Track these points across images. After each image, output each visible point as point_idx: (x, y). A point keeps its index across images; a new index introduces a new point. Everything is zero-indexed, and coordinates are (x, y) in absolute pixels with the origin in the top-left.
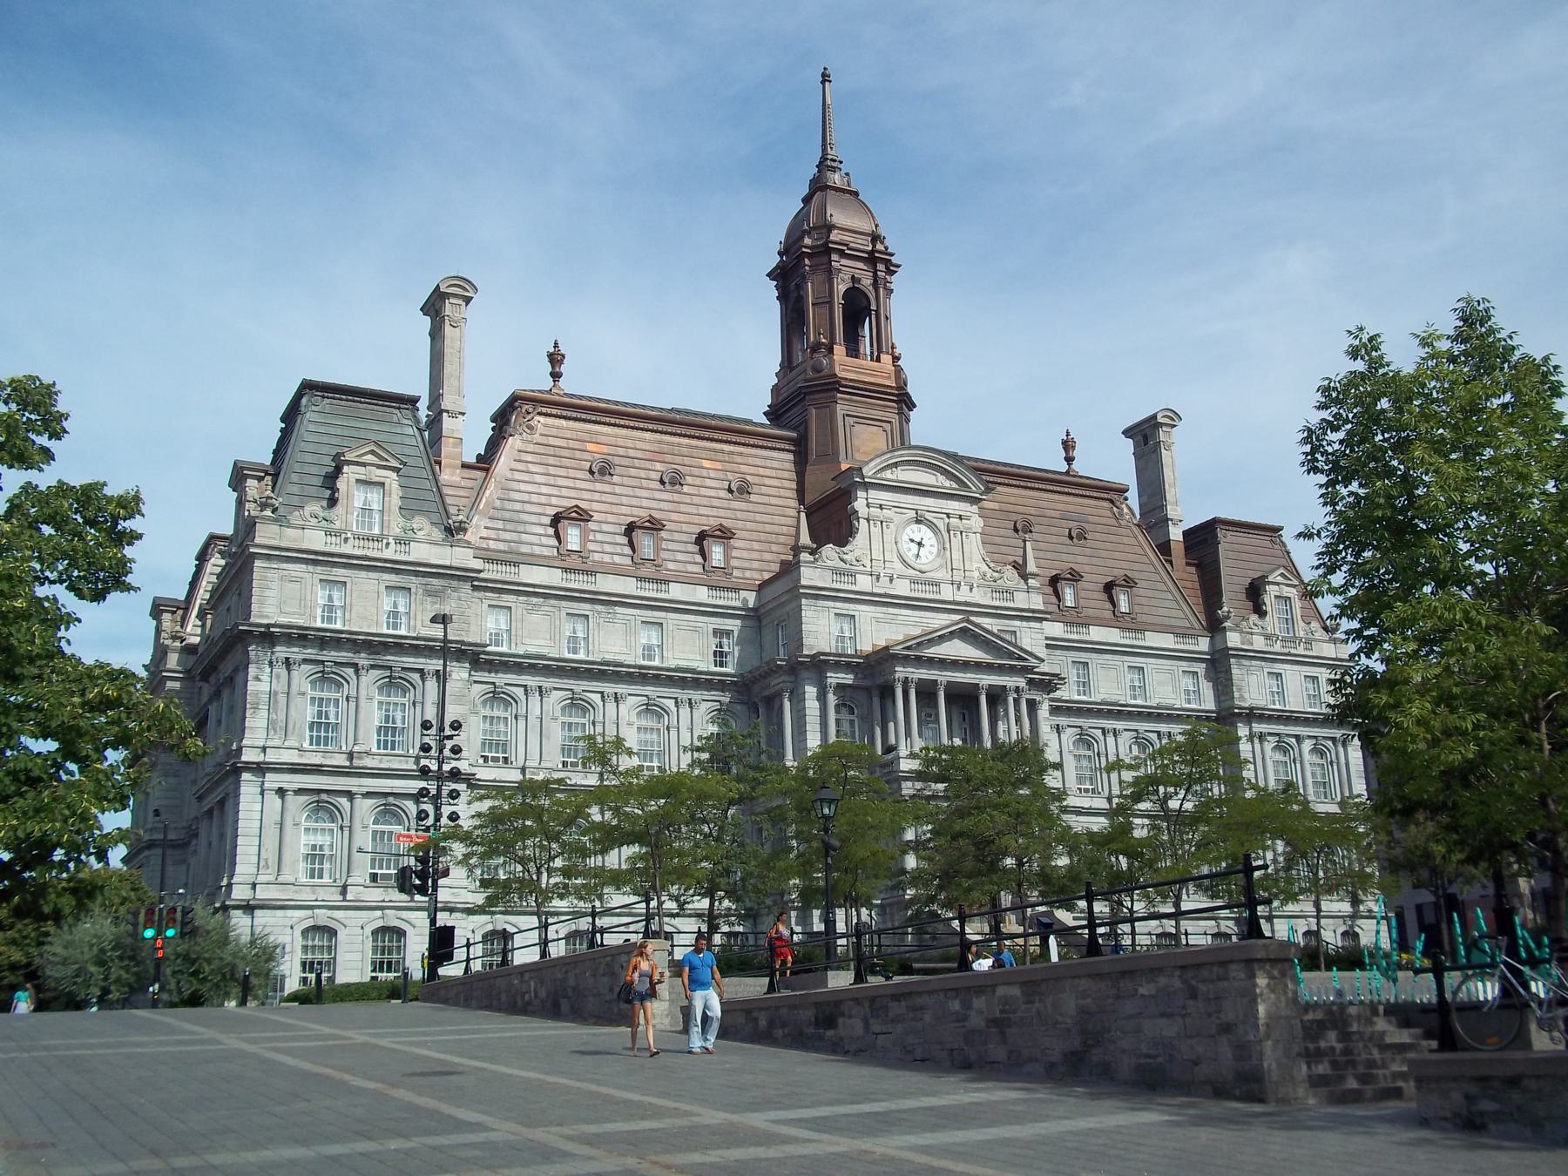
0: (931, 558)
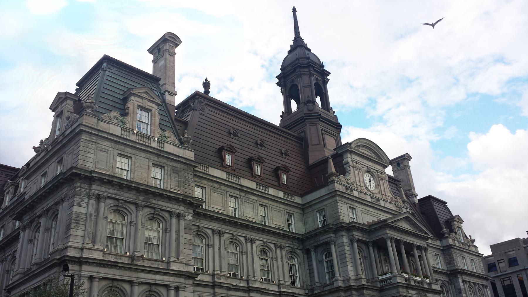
0: (374, 188)
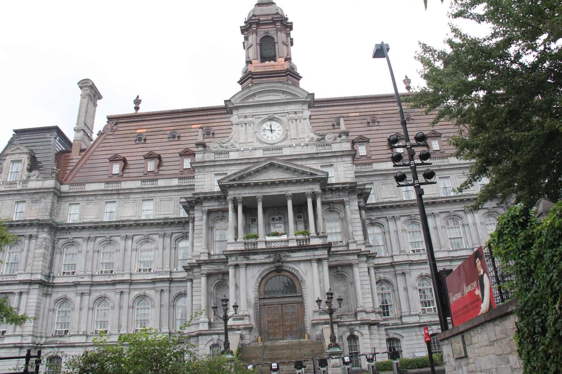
0: (278, 136)
